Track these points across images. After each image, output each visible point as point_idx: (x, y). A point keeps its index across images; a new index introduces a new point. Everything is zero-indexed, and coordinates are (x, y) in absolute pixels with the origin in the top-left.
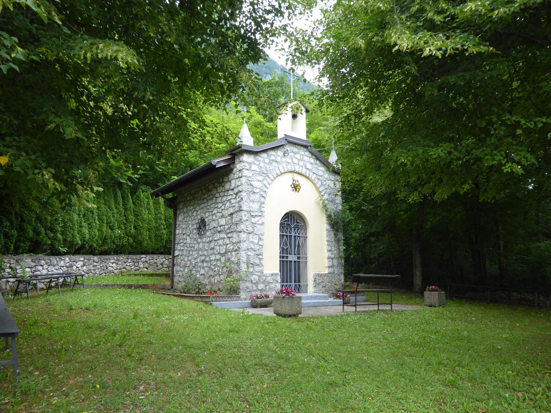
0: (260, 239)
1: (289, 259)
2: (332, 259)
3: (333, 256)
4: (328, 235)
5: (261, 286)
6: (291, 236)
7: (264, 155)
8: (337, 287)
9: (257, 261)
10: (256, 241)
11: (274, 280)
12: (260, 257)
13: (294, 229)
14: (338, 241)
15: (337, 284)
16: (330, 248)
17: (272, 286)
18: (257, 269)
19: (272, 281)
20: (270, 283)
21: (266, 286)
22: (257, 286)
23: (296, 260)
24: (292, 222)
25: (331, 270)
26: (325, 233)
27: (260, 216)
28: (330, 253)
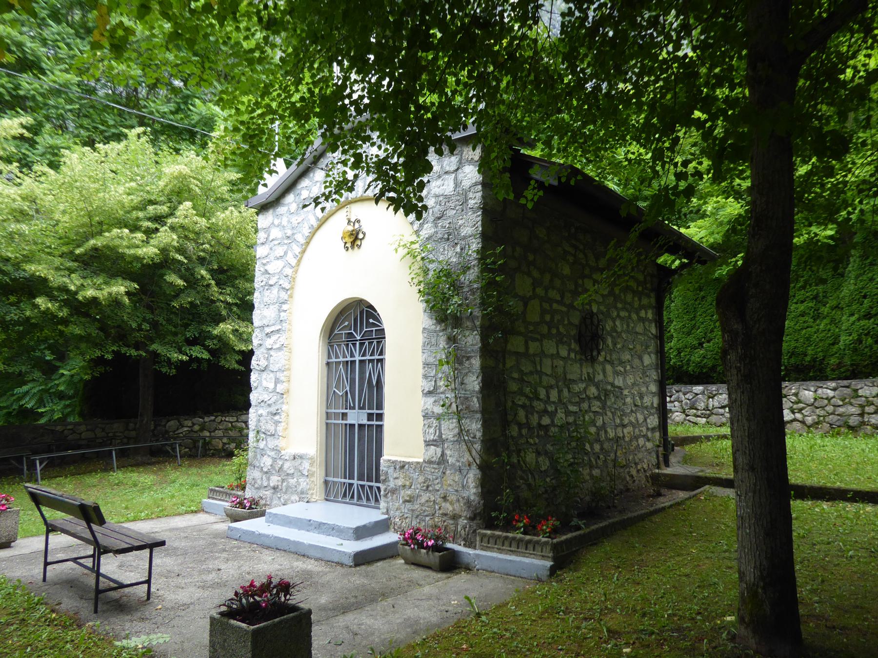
0: (277, 381)
1: (350, 421)
2: (439, 418)
3: (438, 410)
4: (427, 345)
5: (275, 480)
6: (353, 362)
7: (290, 198)
8: (448, 507)
9: (271, 428)
10: (271, 386)
11: (296, 468)
12: (277, 418)
13: (362, 345)
14: (457, 359)
15: (452, 497)
16: (429, 386)
17: (293, 481)
18: (272, 443)
19: (292, 472)
20: (288, 475)
21: (283, 481)
22: (268, 479)
23: (365, 421)
24: (355, 327)
25: (434, 452)
26: (420, 339)
27: (278, 331)
28: (431, 400)
